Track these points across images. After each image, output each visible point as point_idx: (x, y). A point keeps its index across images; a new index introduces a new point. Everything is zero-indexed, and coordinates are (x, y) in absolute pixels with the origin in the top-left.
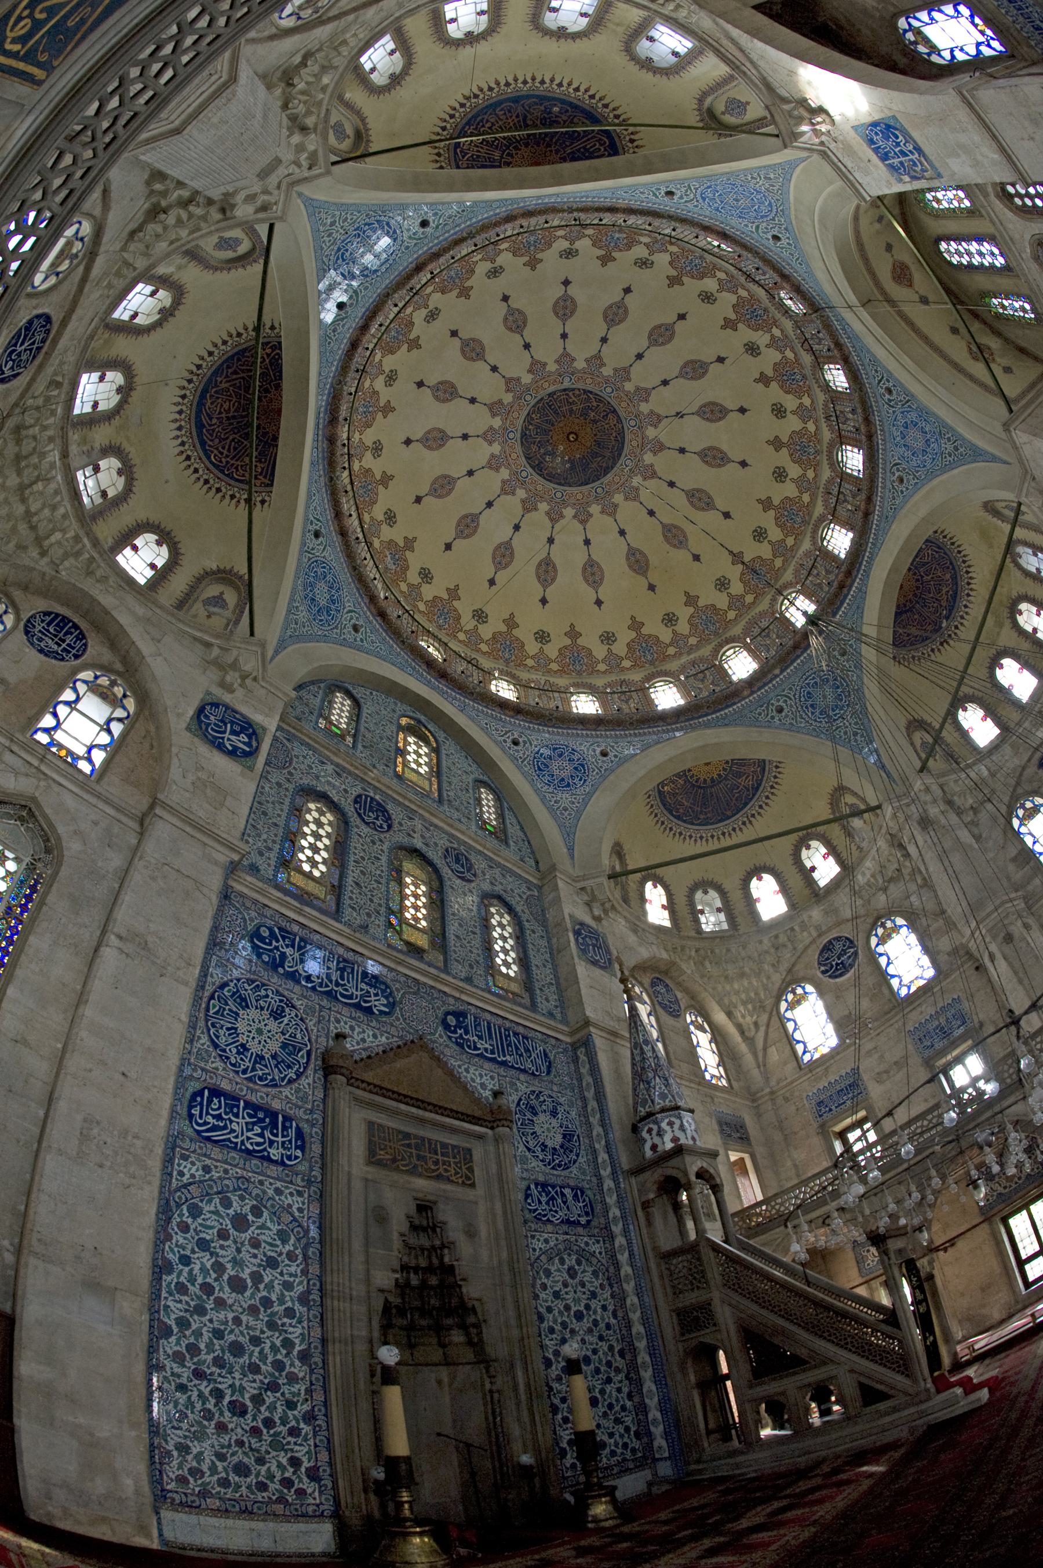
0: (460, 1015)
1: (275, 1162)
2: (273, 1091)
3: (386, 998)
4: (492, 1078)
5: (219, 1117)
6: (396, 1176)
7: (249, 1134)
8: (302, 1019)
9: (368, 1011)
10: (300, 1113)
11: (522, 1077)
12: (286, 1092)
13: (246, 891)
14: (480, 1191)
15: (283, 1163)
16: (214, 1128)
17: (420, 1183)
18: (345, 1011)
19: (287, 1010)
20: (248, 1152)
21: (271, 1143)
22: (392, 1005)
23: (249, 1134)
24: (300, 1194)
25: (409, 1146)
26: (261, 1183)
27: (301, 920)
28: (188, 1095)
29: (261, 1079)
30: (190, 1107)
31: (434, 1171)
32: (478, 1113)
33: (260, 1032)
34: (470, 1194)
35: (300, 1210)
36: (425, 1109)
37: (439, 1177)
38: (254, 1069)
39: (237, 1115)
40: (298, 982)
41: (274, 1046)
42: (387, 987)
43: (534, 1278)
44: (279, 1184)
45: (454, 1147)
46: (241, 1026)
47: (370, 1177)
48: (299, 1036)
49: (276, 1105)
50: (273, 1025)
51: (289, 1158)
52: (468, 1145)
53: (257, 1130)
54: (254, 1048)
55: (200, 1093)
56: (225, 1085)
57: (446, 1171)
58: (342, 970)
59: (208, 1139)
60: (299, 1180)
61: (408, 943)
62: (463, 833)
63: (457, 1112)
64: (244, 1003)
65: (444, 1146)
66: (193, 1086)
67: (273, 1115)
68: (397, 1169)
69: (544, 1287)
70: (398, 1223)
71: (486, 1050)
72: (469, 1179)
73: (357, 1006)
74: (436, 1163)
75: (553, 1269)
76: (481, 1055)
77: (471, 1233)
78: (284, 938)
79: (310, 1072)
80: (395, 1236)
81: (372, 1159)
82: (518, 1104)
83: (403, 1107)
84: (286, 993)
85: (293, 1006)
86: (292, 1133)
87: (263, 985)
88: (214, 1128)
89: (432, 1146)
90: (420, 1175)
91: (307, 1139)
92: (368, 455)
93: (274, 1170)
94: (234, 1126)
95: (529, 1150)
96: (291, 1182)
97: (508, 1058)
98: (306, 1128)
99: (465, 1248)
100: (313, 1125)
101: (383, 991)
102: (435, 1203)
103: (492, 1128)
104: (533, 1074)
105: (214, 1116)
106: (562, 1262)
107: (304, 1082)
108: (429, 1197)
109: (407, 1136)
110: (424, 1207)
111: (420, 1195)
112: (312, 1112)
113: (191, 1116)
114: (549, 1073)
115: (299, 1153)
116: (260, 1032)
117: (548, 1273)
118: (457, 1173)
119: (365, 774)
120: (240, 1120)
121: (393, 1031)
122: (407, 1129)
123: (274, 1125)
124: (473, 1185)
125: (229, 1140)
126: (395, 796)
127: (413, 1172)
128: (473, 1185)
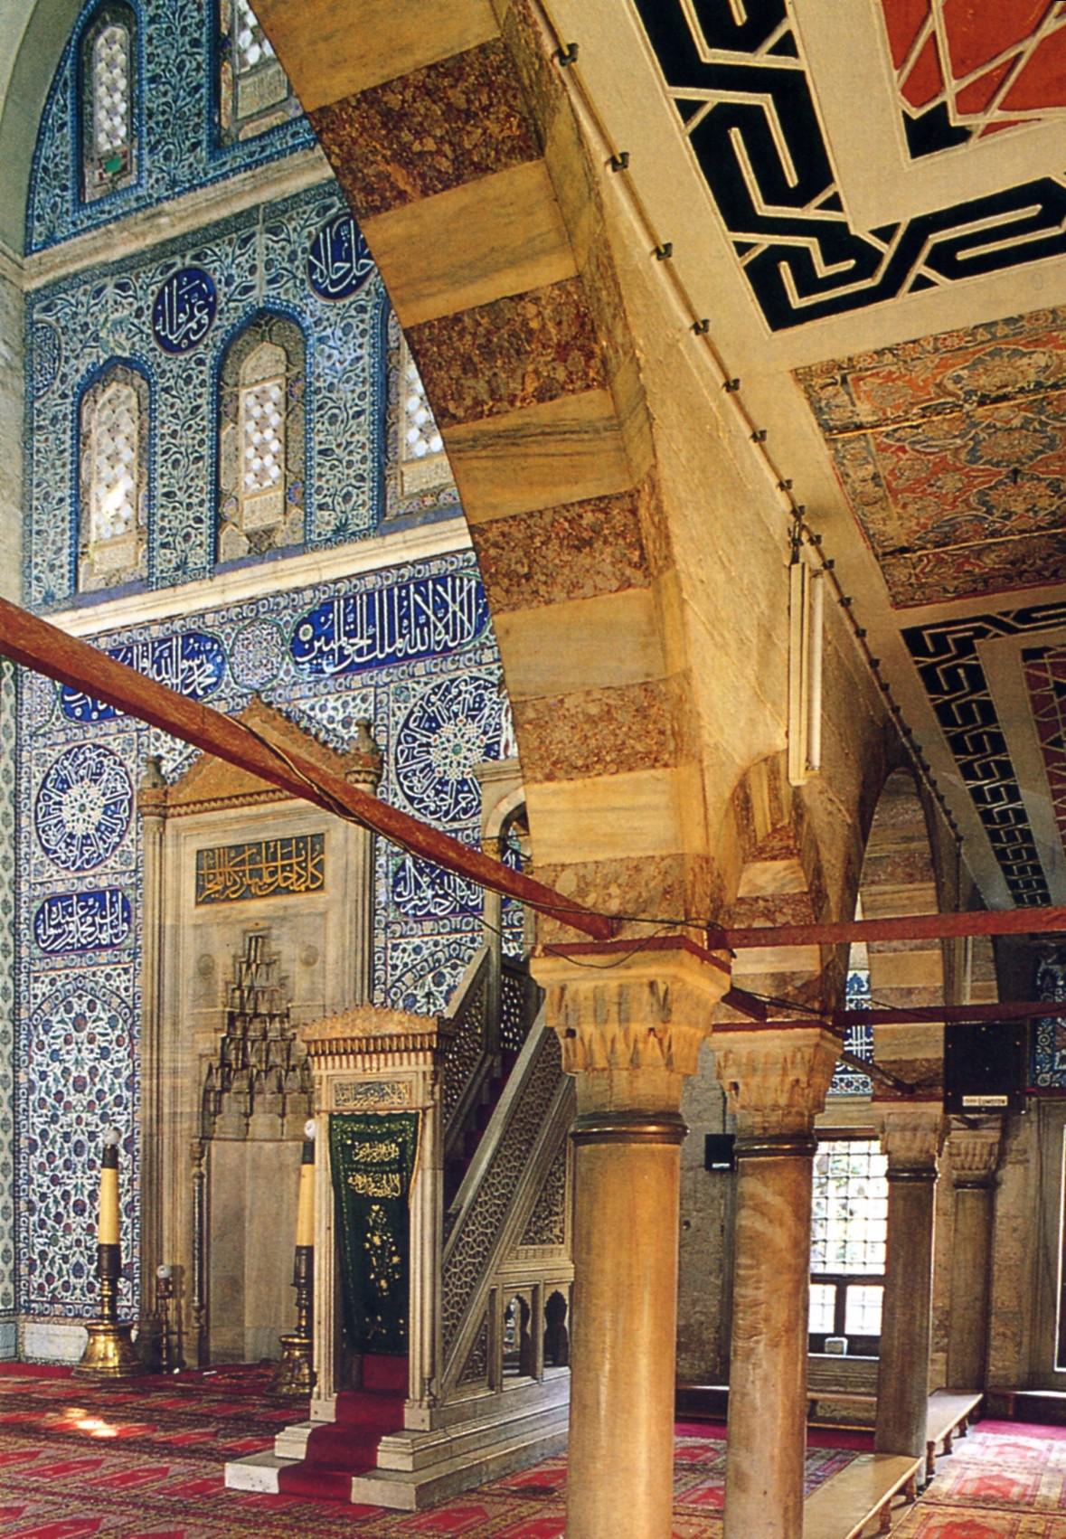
1: (106, 946)
2: (99, 869)
4: (364, 700)
5: (59, 925)
7: (83, 928)
8: (121, 764)
10: (125, 880)
11: (420, 668)
12: (110, 863)
14: (332, 890)
15: (112, 945)
16: (58, 936)
19: (106, 762)
20: (83, 947)
21: (101, 926)
23: (83, 928)
24: (126, 971)
25: (242, 862)
26: (94, 974)
29: (88, 862)
30: (36, 928)
33: (82, 808)
35: (126, 989)
37: (278, 891)
39: (71, 915)
41: (97, 815)
42: (214, 641)
44: (108, 969)
46: (66, 814)
49: (103, 883)
50: (94, 792)
51: (117, 936)
53: (89, 919)
54: (80, 830)
55: (42, 910)
56: (60, 889)
57: (286, 879)
59: (52, 952)
64: (64, 785)
66: (38, 904)
67: (99, 895)
68: (228, 899)
71: (360, 653)
74: (272, 874)
76: (355, 668)
77: (311, 959)
79: (132, 825)
80: (221, 986)
81: (204, 898)
82: (406, 725)
85: (112, 753)
86: (119, 907)
87: (80, 747)
88: (58, 936)
91: (133, 905)
93: (105, 956)
94: (72, 927)
99: (300, 983)
104: (447, 649)
105: (55, 927)
107: (126, 841)
108: (263, 924)
109: (239, 848)
111: (250, 925)
112: (136, 871)
113: (37, 936)
114: (478, 631)
115: (125, 927)
116: (82, 808)
120: (76, 918)
123: (103, 907)
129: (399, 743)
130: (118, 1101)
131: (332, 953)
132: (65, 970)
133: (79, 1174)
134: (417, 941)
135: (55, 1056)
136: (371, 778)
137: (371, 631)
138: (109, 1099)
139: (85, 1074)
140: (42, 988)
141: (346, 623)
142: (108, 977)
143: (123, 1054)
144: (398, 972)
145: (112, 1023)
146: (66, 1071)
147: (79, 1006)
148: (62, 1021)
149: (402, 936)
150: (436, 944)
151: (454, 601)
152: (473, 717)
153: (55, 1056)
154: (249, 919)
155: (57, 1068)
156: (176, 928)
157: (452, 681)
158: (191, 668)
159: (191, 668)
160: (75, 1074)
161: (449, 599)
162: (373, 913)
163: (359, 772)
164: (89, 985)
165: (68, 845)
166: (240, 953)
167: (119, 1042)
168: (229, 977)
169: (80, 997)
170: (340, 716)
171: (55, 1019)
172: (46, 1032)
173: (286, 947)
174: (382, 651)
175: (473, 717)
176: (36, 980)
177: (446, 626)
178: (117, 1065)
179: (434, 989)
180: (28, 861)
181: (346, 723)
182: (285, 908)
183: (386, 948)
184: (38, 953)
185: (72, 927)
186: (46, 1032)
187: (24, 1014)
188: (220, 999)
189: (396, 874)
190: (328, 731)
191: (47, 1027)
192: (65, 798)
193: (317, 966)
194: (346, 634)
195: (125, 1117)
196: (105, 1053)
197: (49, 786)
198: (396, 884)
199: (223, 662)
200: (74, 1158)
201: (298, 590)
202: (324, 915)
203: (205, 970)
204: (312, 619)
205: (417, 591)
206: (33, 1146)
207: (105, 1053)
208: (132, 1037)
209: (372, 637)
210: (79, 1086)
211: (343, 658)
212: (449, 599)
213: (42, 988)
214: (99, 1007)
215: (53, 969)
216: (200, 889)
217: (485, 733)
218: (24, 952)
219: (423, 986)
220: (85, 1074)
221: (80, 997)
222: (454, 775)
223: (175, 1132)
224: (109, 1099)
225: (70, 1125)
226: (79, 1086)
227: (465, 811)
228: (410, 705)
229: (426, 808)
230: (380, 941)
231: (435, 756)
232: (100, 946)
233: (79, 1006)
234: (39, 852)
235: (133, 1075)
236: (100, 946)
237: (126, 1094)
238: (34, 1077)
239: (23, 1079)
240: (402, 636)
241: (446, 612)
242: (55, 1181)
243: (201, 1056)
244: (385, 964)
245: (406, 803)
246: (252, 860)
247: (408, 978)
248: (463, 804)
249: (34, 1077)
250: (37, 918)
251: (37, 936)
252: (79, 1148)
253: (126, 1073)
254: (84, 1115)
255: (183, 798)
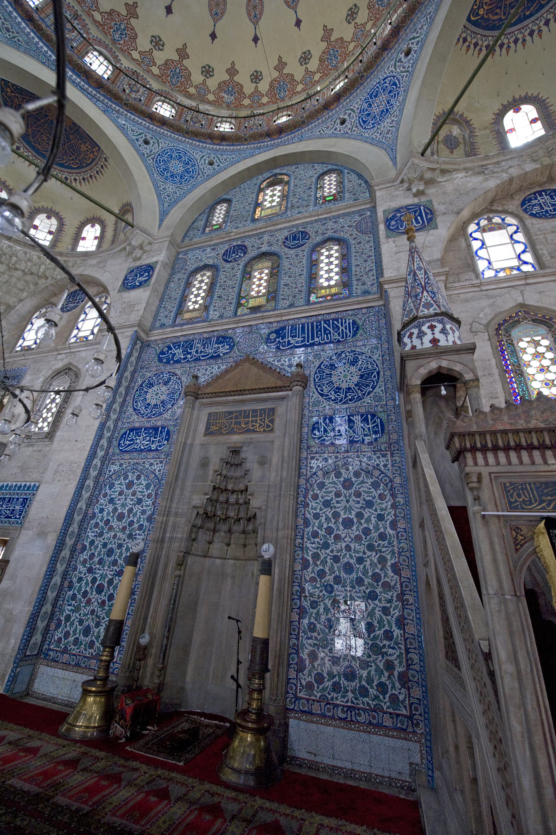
0: (280, 332)
1: (154, 450)
2: (158, 418)
3: (229, 345)
5: (132, 440)
6: (221, 438)
8: (179, 379)
9: (219, 356)
13: (157, 338)
17: (236, 438)
18: (204, 363)
19: (172, 378)
20: (142, 450)
21: (153, 441)
22: (232, 348)
24: (161, 462)
25: (231, 418)
27: (184, 333)
28: (120, 436)
29: (154, 415)
30: (120, 441)
31: (244, 428)
32: (279, 383)
33: (157, 394)
34: (270, 436)
35: (159, 471)
36: (243, 394)
37: (248, 431)
38: (152, 411)
40: (180, 362)
42: (230, 338)
43: (307, 490)
44: (152, 461)
45: (261, 410)
47: (205, 442)
48: (176, 387)
49: (159, 423)
50: (164, 388)
51: (160, 446)
52: (274, 406)
54: (153, 402)
55: (125, 433)
56: (137, 425)
57: (253, 426)
58: (204, 345)
59: (125, 451)
60: (163, 457)
61: (250, 308)
62: (299, 219)
63: (264, 389)
64: (151, 385)
65: (254, 411)
66: (123, 431)
67: (156, 429)
69: (315, 497)
70: (215, 464)
72: (268, 426)
73: (212, 357)
74: (246, 424)
75: (327, 481)
77: (263, 462)
78: (174, 347)
80: (211, 472)
81: (208, 432)
83: (230, 398)
84: (173, 371)
85: (176, 375)
86: (164, 434)
88: (129, 445)
89: (246, 414)
90: (235, 433)
91: (171, 434)
92: (156, 53)
93: (152, 454)
94: (138, 441)
95: (322, 395)
96: (159, 458)
97: (316, 339)
98: (172, 429)
99: (256, 473)
100: (176, 426)
101: (227, 342)
102: (241, 447)
103: (291, 390)
104: (339, 341)
106: (338, 475)
108: (238, 445)
109: (231, 413)
110: (235, 452)
111: (233, 445)
112: (177, 419)
113: (119, 444)
114: (354, 335)
116: (157, 394)
117: (321, 486)
118: (261, 425)
119: (230, 236)
120: (142, 437)
121: (231, 360)
122: (232, 410)
124: (272, 430)
125: (134, 448)
126: (250, 233)
127: (231, 432)
128: (272, 430)
129: (316, 373)
130: (141, 527)
131: (275, 460)
132: (128, 460)
133: (106, 568)
134: (326, 456)
135: (111, 501)
136: (303, 385)
137: (303, 335)
138: (136, 526)
139: (125, 511)
140: (114, 468)
141: (291, 333)
142: (151, 464)
143: (149, 502)
144: (314, 470)
145: (148, 487)
146: (115, 509)
147: (131, 477)
148: (121, 484)
149: (316, 453)
150: (336, 457)
151: (342, 325)
152: (353, 365)
153: (111, 501)
154: (232, 443)
155: (111, 508)
156: (192, 445)
157: (342, 352)
158: (219, 347)
159: (219, 347)
160: (119, 511)
161: (340, 325)
162: (301, 441)
163: (298, 381)
164: (140, 468)
165: (146, 407)
166: (224, 457)
167: (149, 496)
168: (216, 468)
169: (133, 473)
170: (287, 364)
171: (117, 483)
172: (110, 489)
173: (250, 456)
174: (308, 341)
175: (353, 365)
176: (113, 464)
177: (339, 334)
178: (144, 508)
179: (335, 480)
180: (125, 413)
181: (290, 366)
182: (251, 439)
183: (307, 458)
184: (117, 451)
185: (138, 441)
186: (110, 489)
187: (101, 479)
188: (210, 478)
189: (314, 425)
190: (280, 369)
191: (112, 486)
192: (150, 390)
193: (266, 466)
194: (291, 336)
195: (142, 537)
196: (139, 501)
197: (144, 385)
198: (314, 429)
199: (234, 345)
200: (106, 558)
201: (270, 323)
202: (272, 442)
203: (205, 463)
204: (276, 332)
205: (325, 323)
206: (84, 548)
207: (139, 501)
208: (156, 494)
209: (304, 337)
210: (121, 517)
211: (289, 343)
212: (340, 325)
213: (114, 468)
214: (142, 477)
215: (122, 459)
216: (207, 428)
217: (360, 370)
218: (111, 451)
219: (329, 478)
220: (125, 511)
221: (133, 473)
222: (344, 386)
223: (170, 547)
224: (136, 526)
225: (109, 539)
226: (121, 517)
227: (351, 400)
228: (321, 360)
229: (330, 398)
230: (304, 455)
231: (334, 379)
232: (151, 450)
233: (131, 477)
234: (131, 410)
235: (153, 514)
236: (151, 450)
237: (146, 524)
238: (96, 511)
239: (90, 512)
240: (317, 337)
241: (339, 329)
242: (90, 570)
243: (195, 507)
244: (306, 466)
245: (319, 396)
246: (236, 417)
247: (320, 473)
248: (350, 397)
249: (96, 511)
250: (122, 436)
251: (119, 444)
252: (110, 552)
253: (149, 513)
254: (118, 534)
255: (207, 391)
